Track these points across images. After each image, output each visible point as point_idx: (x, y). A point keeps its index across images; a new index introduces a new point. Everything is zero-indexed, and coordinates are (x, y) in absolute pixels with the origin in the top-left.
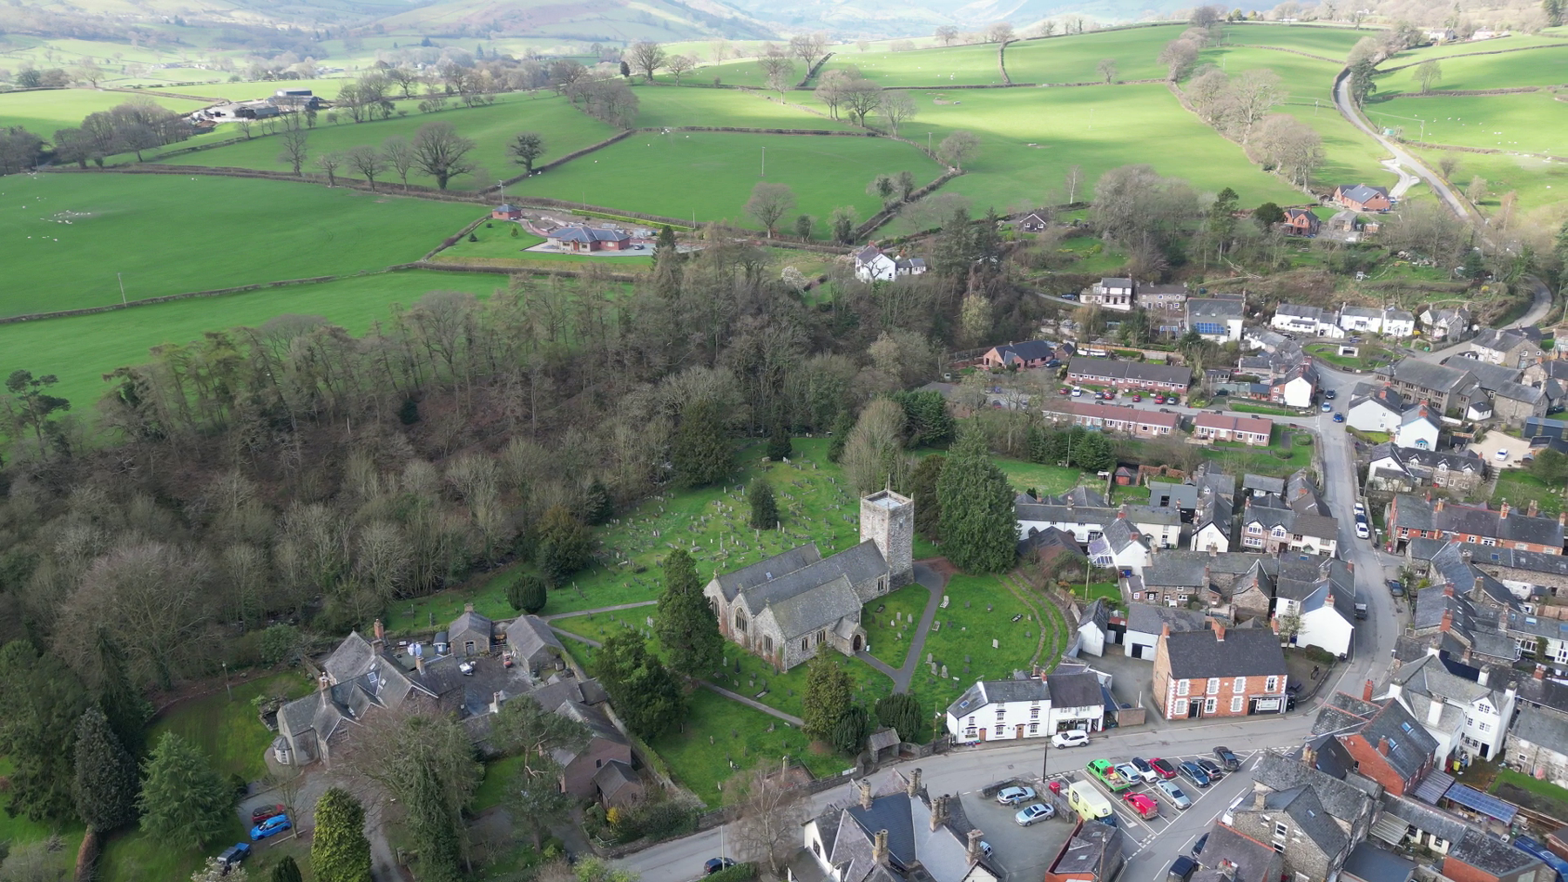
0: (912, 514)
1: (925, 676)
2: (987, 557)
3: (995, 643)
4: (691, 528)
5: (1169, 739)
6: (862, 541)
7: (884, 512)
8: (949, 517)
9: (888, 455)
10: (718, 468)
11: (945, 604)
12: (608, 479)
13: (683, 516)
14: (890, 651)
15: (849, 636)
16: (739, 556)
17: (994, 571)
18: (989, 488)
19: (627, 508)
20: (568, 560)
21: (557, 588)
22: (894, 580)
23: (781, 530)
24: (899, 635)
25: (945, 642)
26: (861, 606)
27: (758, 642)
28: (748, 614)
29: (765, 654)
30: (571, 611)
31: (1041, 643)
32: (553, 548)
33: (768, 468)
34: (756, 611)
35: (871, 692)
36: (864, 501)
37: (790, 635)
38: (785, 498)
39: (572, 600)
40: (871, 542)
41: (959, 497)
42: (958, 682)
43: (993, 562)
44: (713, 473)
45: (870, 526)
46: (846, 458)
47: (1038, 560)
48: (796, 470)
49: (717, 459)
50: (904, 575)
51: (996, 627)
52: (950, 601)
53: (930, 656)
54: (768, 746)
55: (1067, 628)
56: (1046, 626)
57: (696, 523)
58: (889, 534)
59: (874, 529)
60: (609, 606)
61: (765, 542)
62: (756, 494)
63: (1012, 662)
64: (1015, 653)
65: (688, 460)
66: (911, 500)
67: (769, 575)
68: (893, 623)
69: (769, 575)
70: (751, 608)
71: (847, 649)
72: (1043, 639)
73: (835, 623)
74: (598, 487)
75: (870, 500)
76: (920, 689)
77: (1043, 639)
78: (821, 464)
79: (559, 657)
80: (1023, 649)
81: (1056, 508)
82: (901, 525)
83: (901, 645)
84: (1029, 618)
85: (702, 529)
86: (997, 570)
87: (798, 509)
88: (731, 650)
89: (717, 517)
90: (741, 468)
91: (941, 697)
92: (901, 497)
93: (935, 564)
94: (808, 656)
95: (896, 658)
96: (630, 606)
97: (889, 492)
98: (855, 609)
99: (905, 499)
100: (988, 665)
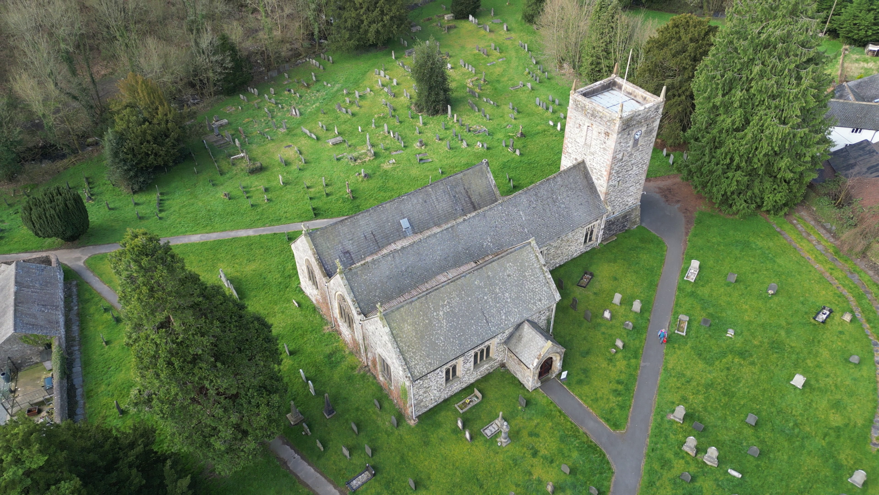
0: (657, 123)
1: (669, 455)
2: (762, 192)
3: (799, 380)
4: (340, 107)
6: (566, 163)
7: (612, 121)
8: (712, 123)
9: (605, 16)
10: (384, 25)
11: (693, 272)
12: (235, 32)
13: (335, 89)
14: (602, 386)
15: (534, 363)
16: (389, 156)
17: (768, 211)
18: (805, 83)
19: (274, 74)
20: (147, 155)
21: (135, 193)
22: (610, 225)
23: (451, 117)
24: (619, 344)
25: (701, 365)
26: (558, 297)
27: (369, 355)
28: (357, 318)
29: (381, 379)
32: (121, 138)
33: (449, 28)
34: (365, 313)
36: (575, 97)
37: (419, 370)
38: (465, 70)
39: (141, 218)
40: (581, 168)
41: (738, 94)
42: (741, 483)
43: (769, 200)
44: (378, 32)
45: (581, 141)
46: (543, 19)
47: (849, 200)
48: (482, 32)
49: (382, 13)
50: (625, 217)
51: (788, 332)
52: (700, 267)
53: (680, 412)
57: (347, 100)
58: (614, 158)
59: (586, 145)
60: (184, 233)
61: (429, 135)
62: (421, 66)
63: (838, 429)
64: (837, 405)
65: (346, 14)
66: (661, 98)
67: (405, 223)
68: (607, 315)
69: (405, 223)
70: (357, 301)
71: (529, 379)
73: (507, 333)
74: (225, 45)
75: (585, 95)
78: (514, 25)
79: (49, 346)
80: (851, 394)
81: (862, 107)
82: (636, 142)
83: (621, 364)
84: (847, 317)
85: (355, 109)
86: (776, 209)
87: (479, 86)
88: (330, 356)
89: (377, 94)
90: (419, 28)
92: (640, 92)
93: (669, 190)
94: (456, 387)
95: (612, 398)
96: (214, 236)
97: (619, 80)
98: (545, 302)
99: (648, 95)
100: (790, 438)
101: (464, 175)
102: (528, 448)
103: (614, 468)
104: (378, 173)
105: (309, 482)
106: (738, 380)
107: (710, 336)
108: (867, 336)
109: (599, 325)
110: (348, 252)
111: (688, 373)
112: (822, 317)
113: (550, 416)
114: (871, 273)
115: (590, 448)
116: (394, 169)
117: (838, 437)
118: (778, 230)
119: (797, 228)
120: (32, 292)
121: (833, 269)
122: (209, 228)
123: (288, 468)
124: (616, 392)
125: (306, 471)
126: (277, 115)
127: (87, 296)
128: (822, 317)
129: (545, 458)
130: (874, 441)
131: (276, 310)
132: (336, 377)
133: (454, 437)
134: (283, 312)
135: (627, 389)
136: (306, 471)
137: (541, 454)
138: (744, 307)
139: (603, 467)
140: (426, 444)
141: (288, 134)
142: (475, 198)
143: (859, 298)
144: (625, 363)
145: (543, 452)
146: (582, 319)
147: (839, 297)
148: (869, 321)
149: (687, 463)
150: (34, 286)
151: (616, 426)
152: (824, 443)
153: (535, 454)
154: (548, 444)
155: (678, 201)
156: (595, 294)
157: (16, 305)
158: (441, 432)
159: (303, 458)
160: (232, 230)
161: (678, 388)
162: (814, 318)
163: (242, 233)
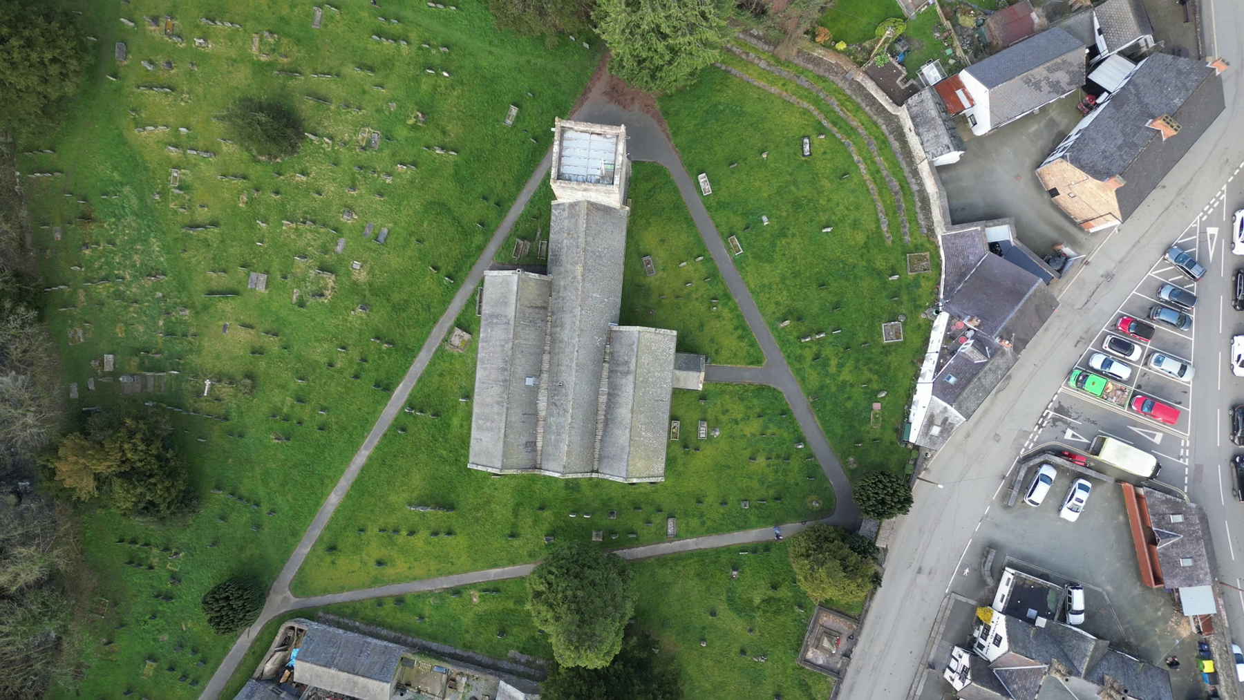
1: (799, 352)
5: (1110, 265)
14: (730, 342)
25: (767, 267)
30: (286, 554)
31: (867, 177)
35: (772, 429)
51: (795, 182)
54: (757, 601)
55: (875, 123)
56: (849, 136)
63: (865, 243)
67: (530, 382)
69: (530, 382)
72: (862, 166)
76: (814, 378)
77: (862, 166)
91: (846, 375)
101: (520, 300)
102: (730, 422)
103: (780, 389)
104: (367, 293)
105: (649, 554)
106: (795, 259)
107: (756, 236)
108: (840, 140)
109: (689, 294)
110: (526, 443)
111: (766, 281)
112: (807, 148)
113: (723, 392)
114: (810, 67)
115: (761, 390)
116: (371, 272)
117: (869, 251)
118: (723, 68)
119: (734, 53)
120: (341, 656)
121: (784, 85)
122: (327, 481)
123: (629, 560)
124: (741, 338)
125: (640, 552)
126: (135, 294)
127: (348, 611)
128: (807, 148)
129: (743, 419)
130: (887, 235)
131: (489, 492)
132: (588, 493)
133: (689, 456)
134: (496, 489)
135: (744, 329)
136: (640, 552)
137: (739, 419)
138: (757, 184)
139: (775, 395)
140: (679, 474)
141: (197, 313)
142: (539, 303)
143: (816, 102)
144: (726, 310)
145: (739, 417)
146: (676, 301)
147: (804, 114)
148: (835, 124)
149: (810, 347)
150: (333, 653)
151: (759, 362)
152: (865, 264)
153: (736, 422)
154: (737, 410)
155: (633, 99)
156: (664, 270)
157: (357, 674)
158: (680, 461)
159: (630, 548)
160: (348, 465)
161: (769, 298)
162: (804, 156)
163: (362, 457)
